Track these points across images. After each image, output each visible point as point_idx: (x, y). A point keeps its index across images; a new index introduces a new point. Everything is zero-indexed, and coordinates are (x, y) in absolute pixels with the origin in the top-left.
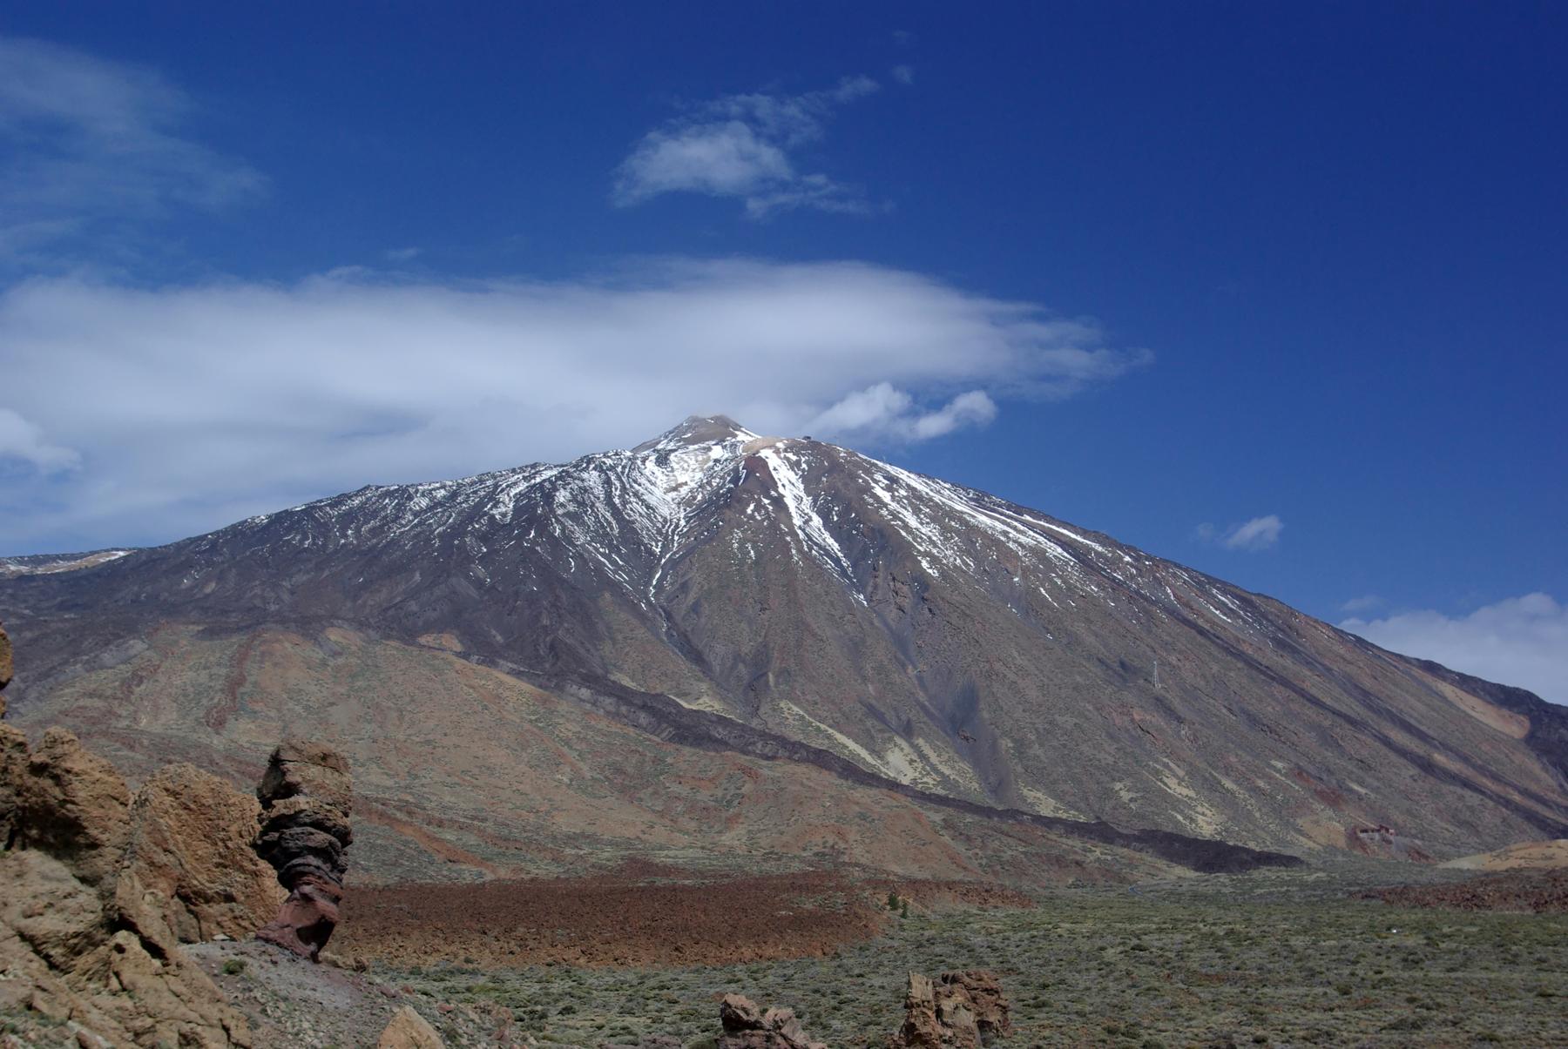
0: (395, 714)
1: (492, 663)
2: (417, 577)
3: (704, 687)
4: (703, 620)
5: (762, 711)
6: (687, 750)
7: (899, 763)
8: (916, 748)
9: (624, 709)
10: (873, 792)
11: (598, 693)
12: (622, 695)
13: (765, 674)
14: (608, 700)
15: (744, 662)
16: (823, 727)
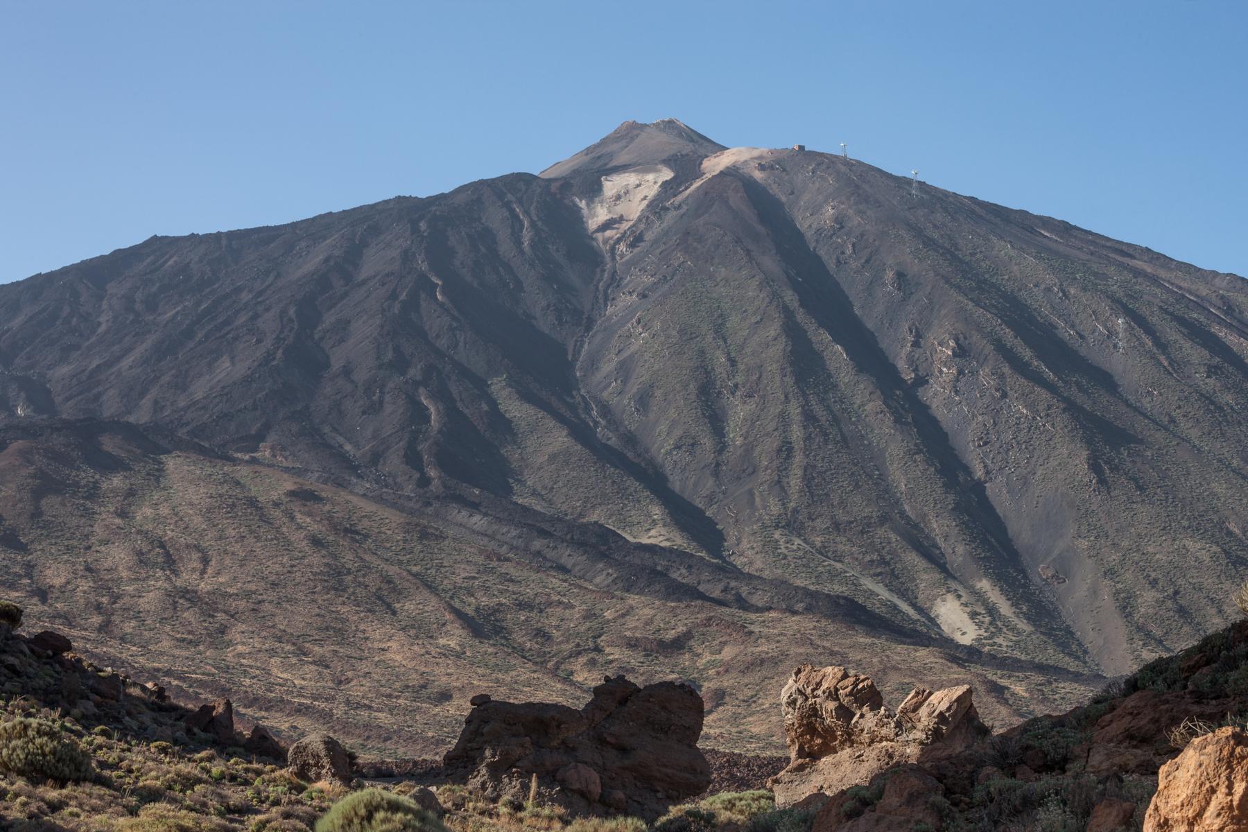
0: (196, 555)
1: (341, 484)
2: (225, 363)
3: (657, 511)
4: (652, 416)
5: (745, 544)
6: (633, 599)
7: (954, 618)
8: (979, 596)
9: (537, 544)
10: (923, 655)
11: (499, 520)
12: (538, 525)
13: (751, 493)
14: (514, 533)
15: (716, 474)
16: (838, 565)
